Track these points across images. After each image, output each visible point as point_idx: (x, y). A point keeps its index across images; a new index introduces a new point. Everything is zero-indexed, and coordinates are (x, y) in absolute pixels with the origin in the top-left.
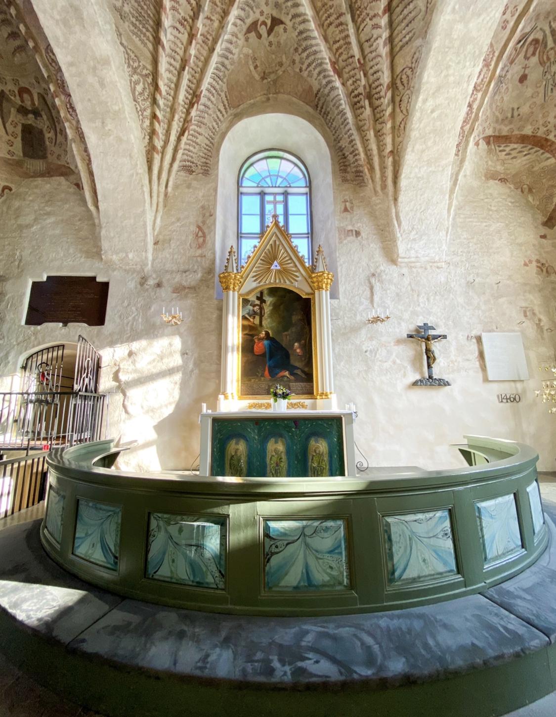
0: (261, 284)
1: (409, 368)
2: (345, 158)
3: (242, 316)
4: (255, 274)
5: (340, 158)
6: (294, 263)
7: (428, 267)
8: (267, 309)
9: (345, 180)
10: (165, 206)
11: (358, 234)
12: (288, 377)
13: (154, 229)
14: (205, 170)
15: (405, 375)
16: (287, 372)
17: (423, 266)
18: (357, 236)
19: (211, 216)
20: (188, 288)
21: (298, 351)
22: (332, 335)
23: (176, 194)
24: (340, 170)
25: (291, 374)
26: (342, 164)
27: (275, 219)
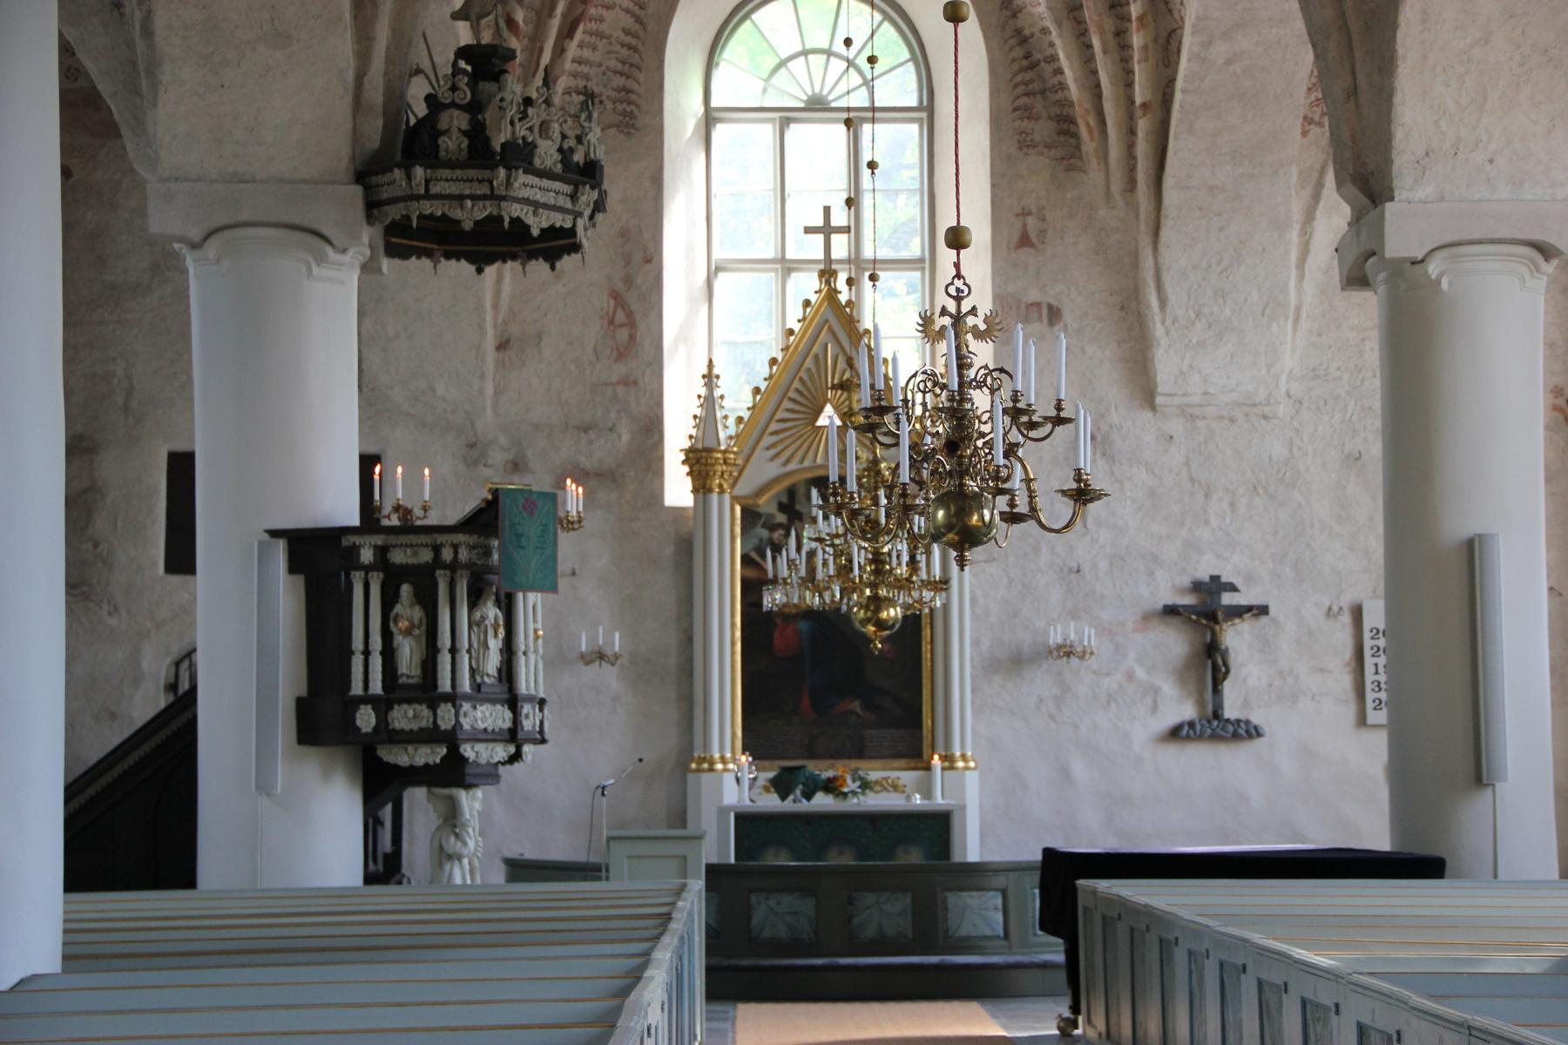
0: (792, 466)
1: (1168, 688)
4: (774, 439)
5: (1015, 67)
7: (1240, 417)
9: (1025, 144)
11: (1054, 314)
12: (858, 715)
13: (496, 307)
14: (624, 114)
15: (1155, 709)
17: (1225, 413)
18: (1051, 324)
19: (649, 261)
20: (596, 474)
22: (973, 601)
24: (1015, 110)
26: (1021, 89)
27: (828, 282)
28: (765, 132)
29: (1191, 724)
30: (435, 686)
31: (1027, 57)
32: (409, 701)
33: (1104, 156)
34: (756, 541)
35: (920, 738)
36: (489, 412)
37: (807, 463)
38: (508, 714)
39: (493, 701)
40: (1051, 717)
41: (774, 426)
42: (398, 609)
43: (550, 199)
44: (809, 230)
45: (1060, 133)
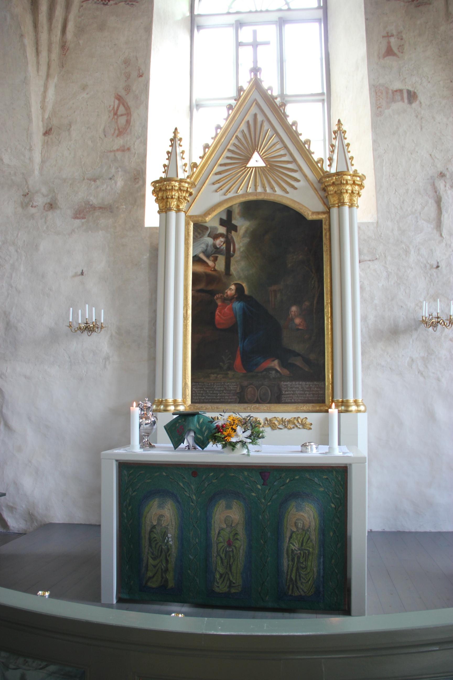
0: (229, 195)
3: (194, 257)
6: (291, 155)
10: (62, 66)
12: (277, 371)
13: (43, 108)
16: (276, 362)
18: (410, 102)
20: (100, 208)
22: (361, 288)
23: (81, 42)
25: (284, 364)
27: (256, 75)
34: (204, 246)
36: (37, 173)
37: (240, 192)
41: (216, 169)
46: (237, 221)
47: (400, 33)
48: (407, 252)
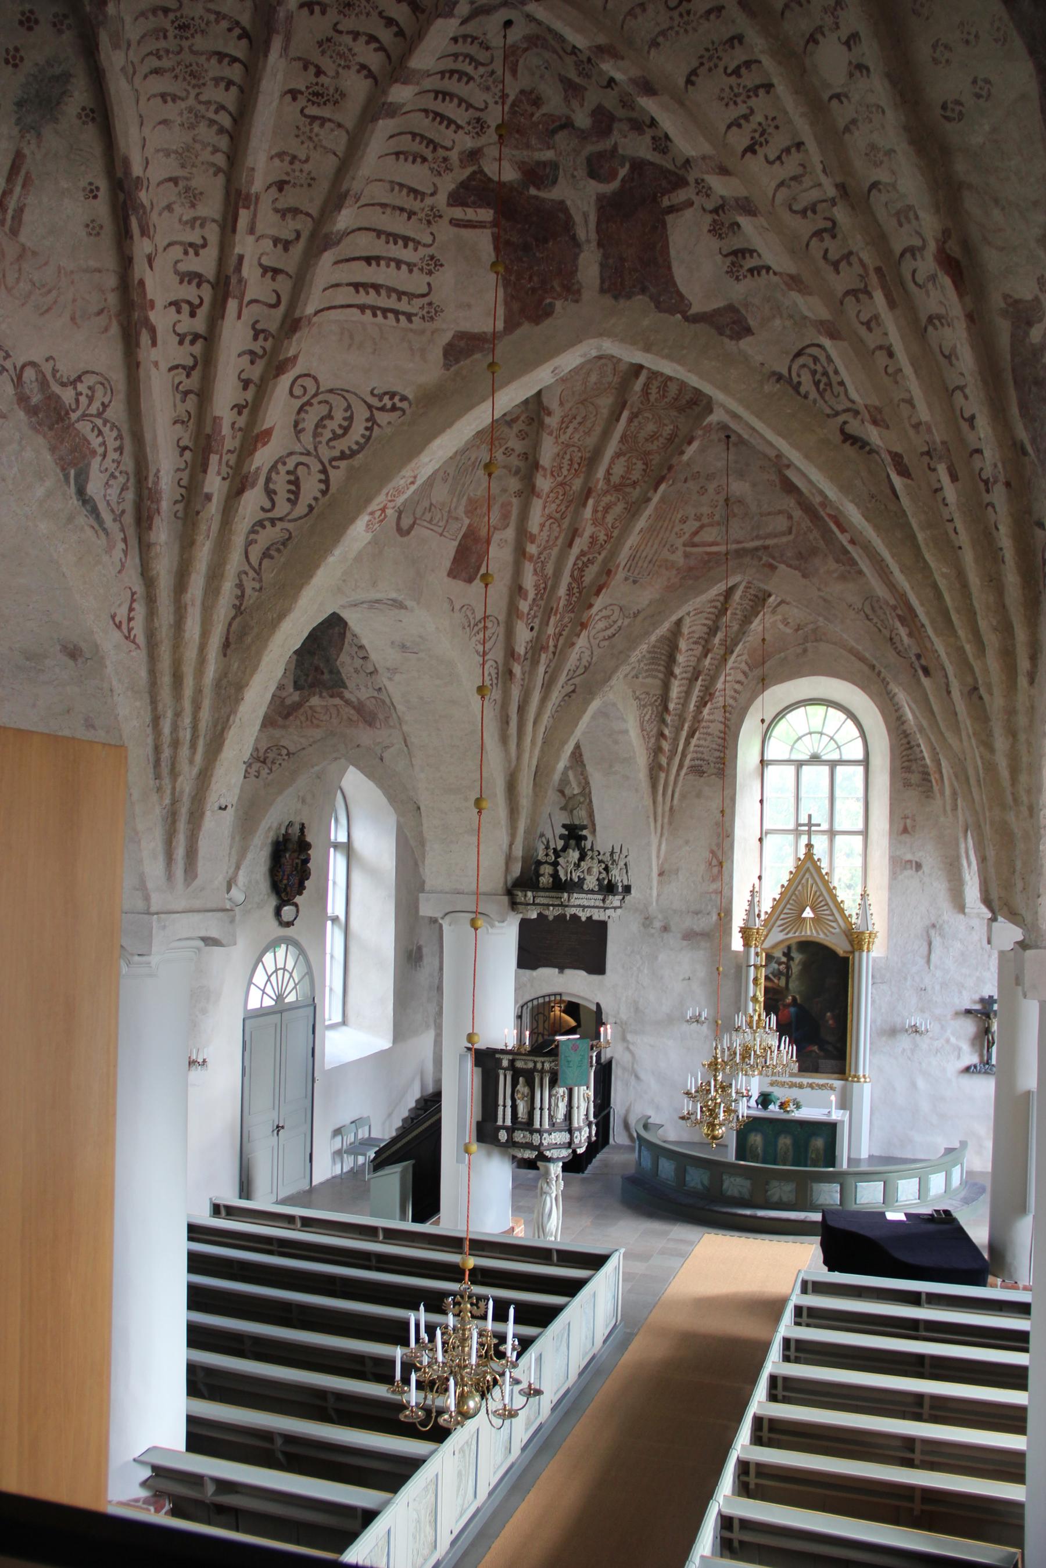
0: (790, 935)
1: (966, 1047)
2: (911, 748)
5: (903, 748)
8: (795, 968)
9: (907, 784)
10: (670, 823)
11: (919, 866)
13: (658, 857)
14: (719, 769)
15: (959, 1057)
21: (831, 1022)
22: (873, 1002)
25: (821, 1048)
26: (905, 758)
28: (791, 769)
29: (975, 1066)
30: (533, 1125)
31: (909, 743)
32: (522, 1130)
33: (942, 793)
35: (845, 1066)
38: (568, 1136)
39: (561, 1131)
40: (909, 1059)
41: (782, 916)
42: (518, 1087)
43: (592, 903)
44: (810, 816)
45: (924, 780)
46: (794, 954)
47: (914, 815)
48: (905, 979)
